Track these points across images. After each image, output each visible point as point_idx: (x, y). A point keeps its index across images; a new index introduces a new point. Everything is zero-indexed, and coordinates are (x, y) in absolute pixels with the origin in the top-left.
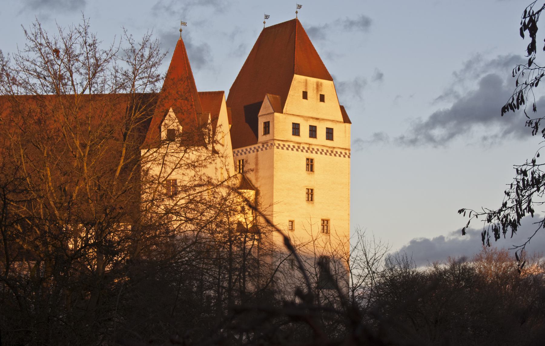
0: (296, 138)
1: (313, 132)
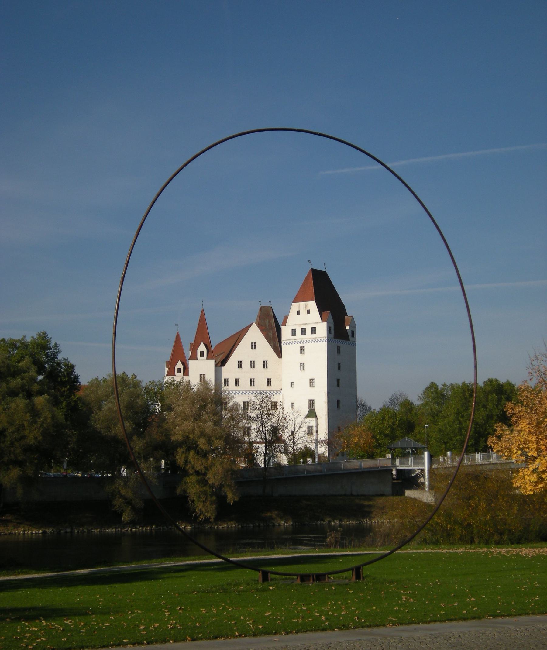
0: (294, 337)
1: (304, 331)
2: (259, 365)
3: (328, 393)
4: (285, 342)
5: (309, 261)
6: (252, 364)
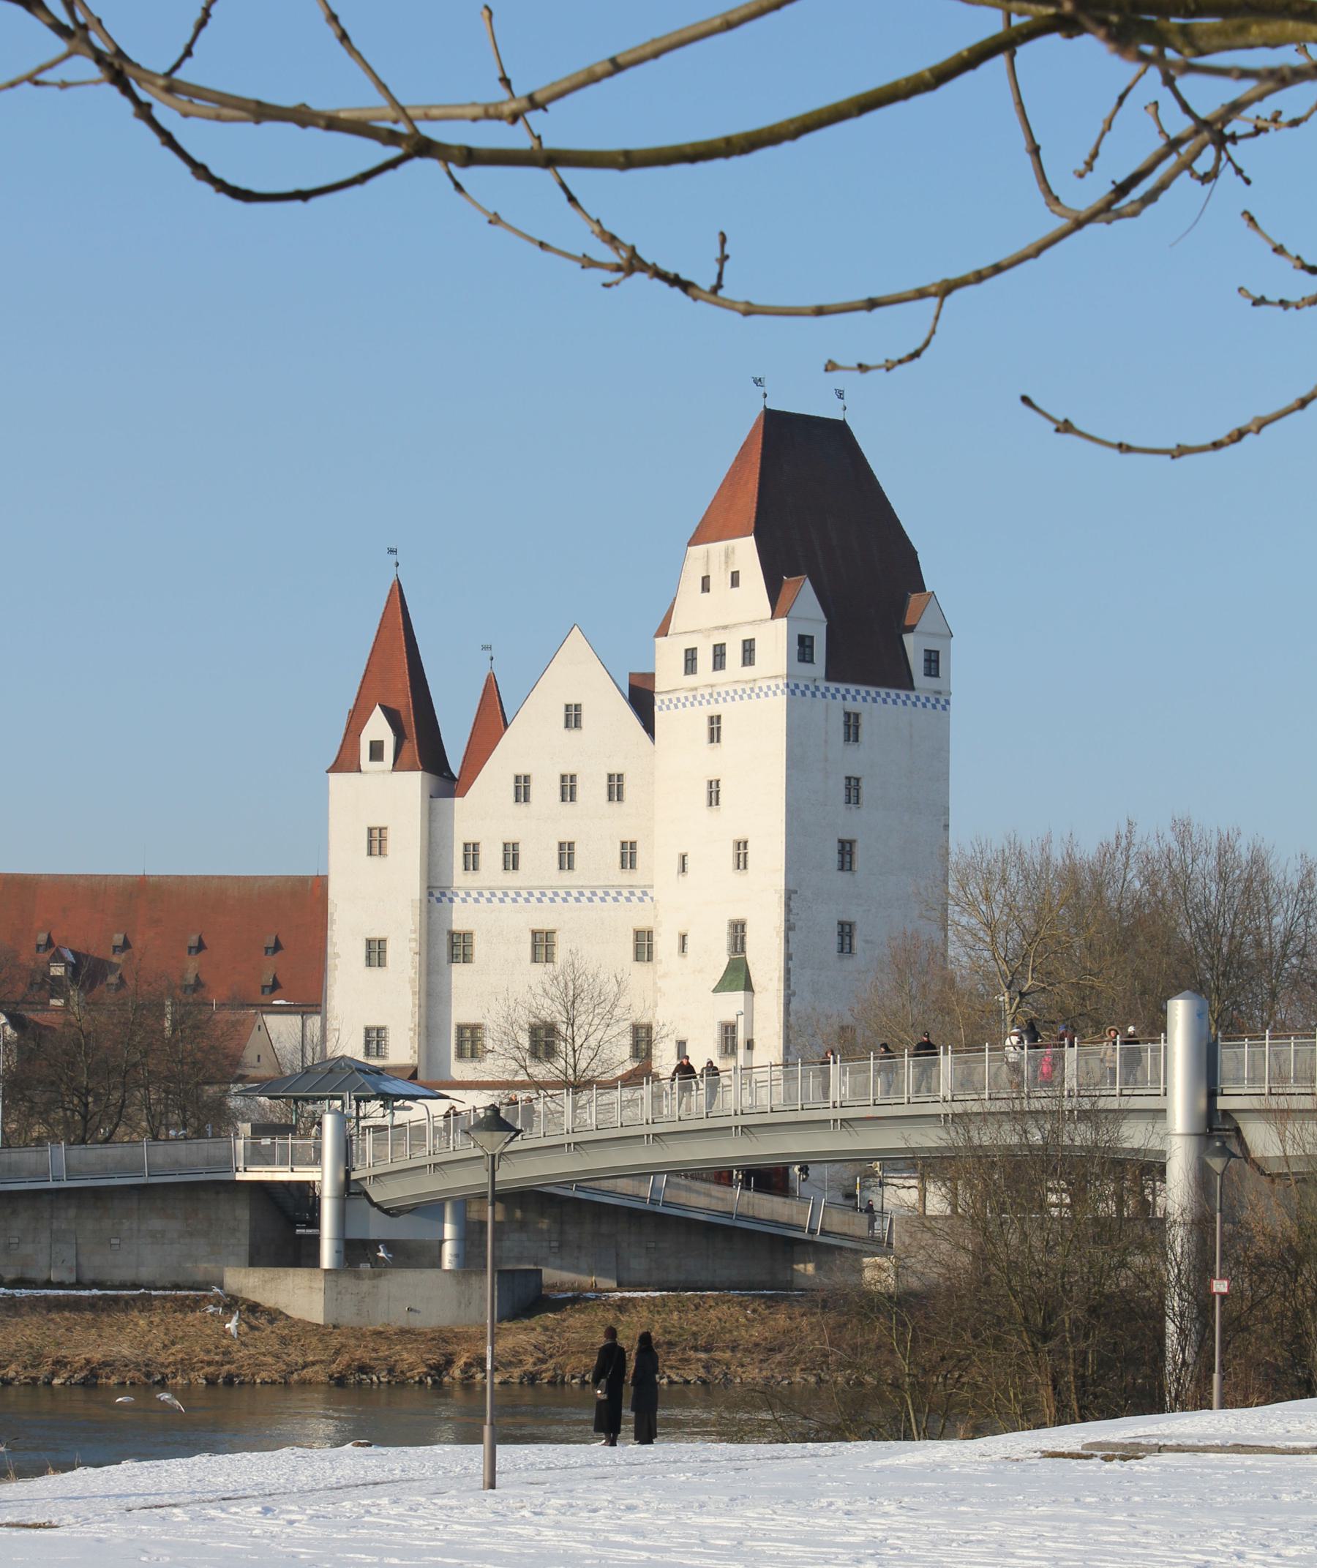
1: (719, 654)
2: (592, 789)
3: (790, 895)
5: (758, 382)
6: (568, 789)
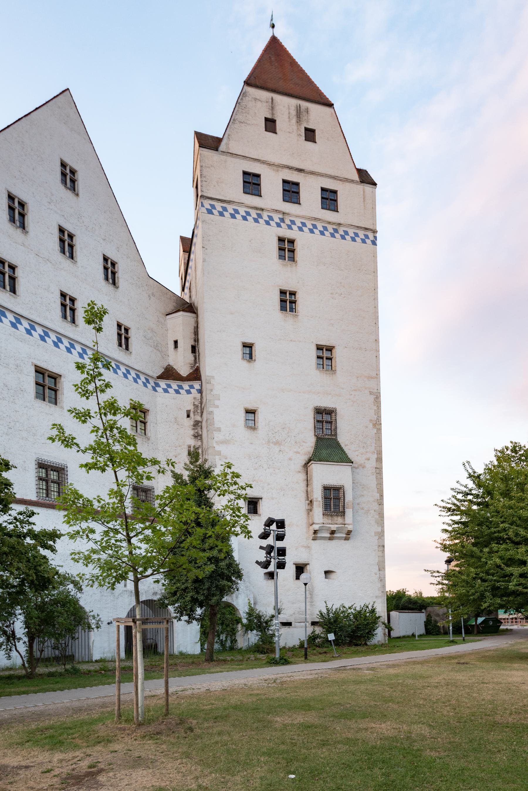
1: (291, 191)
4: (219, 206)
